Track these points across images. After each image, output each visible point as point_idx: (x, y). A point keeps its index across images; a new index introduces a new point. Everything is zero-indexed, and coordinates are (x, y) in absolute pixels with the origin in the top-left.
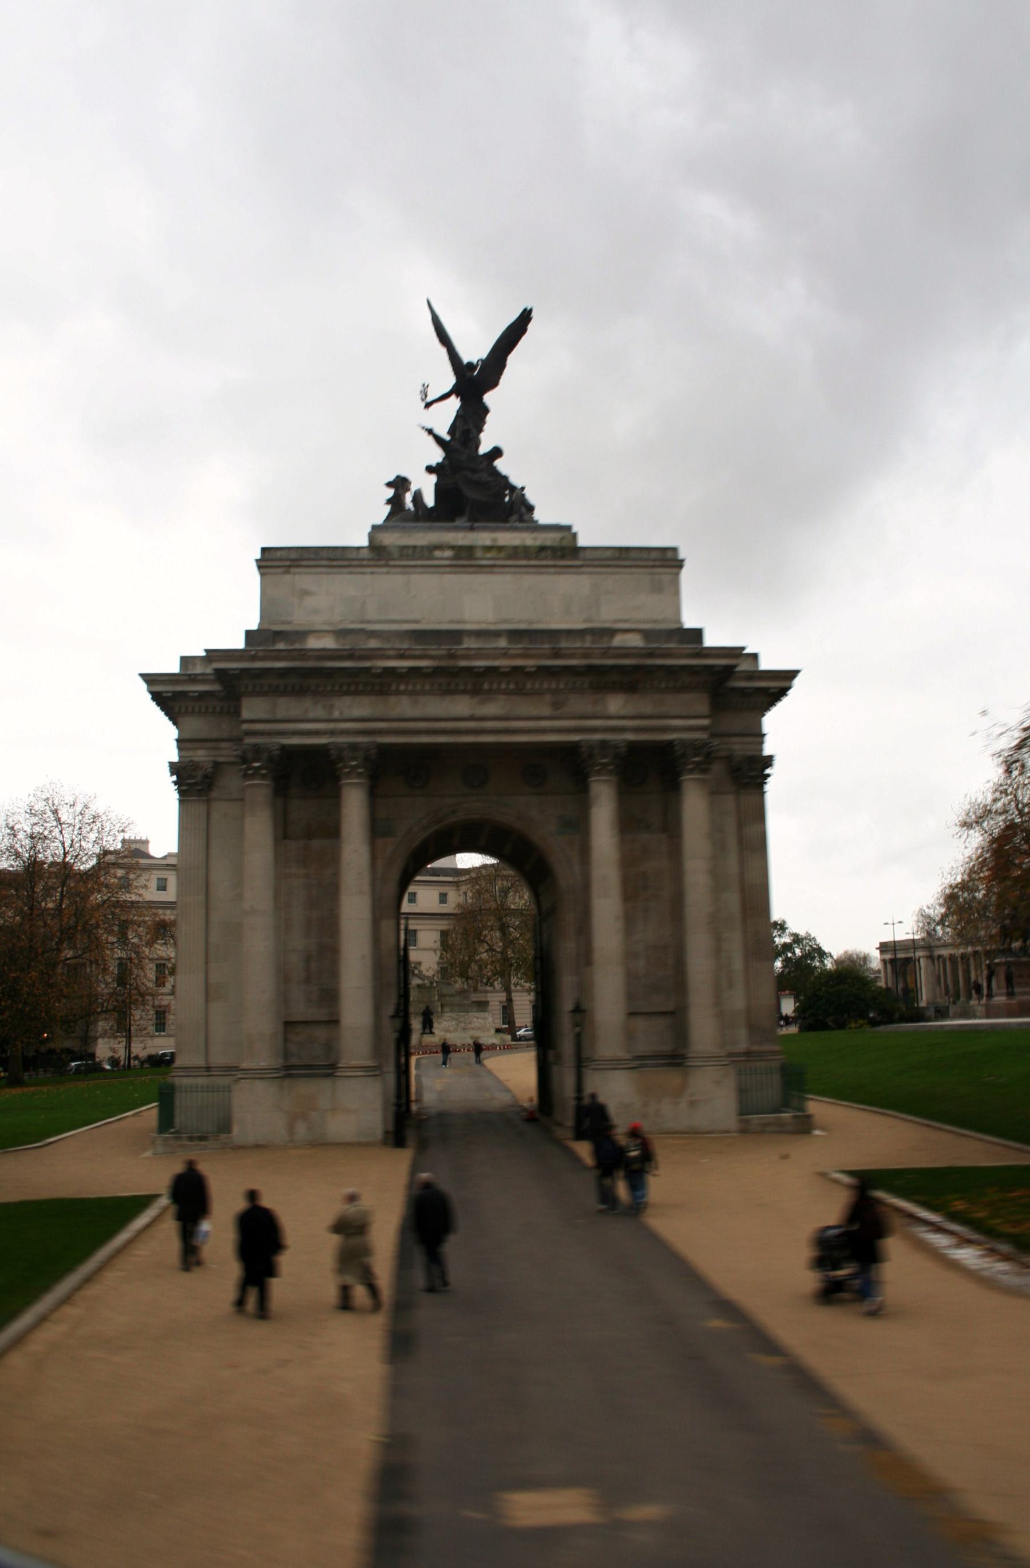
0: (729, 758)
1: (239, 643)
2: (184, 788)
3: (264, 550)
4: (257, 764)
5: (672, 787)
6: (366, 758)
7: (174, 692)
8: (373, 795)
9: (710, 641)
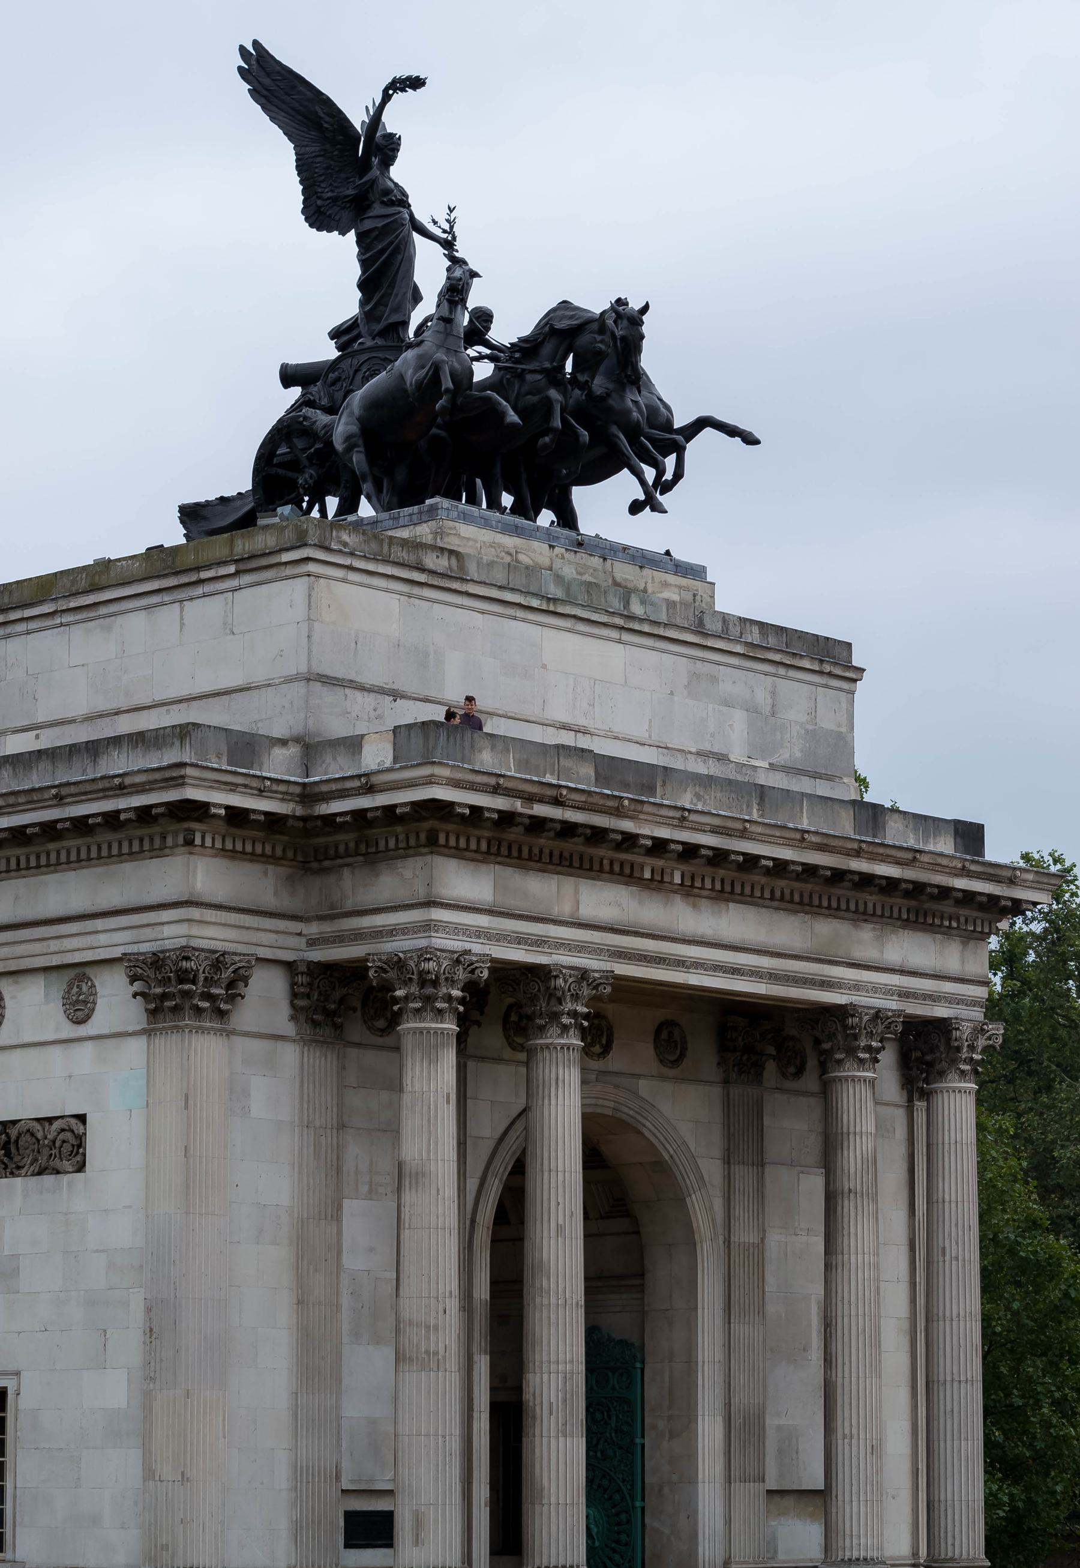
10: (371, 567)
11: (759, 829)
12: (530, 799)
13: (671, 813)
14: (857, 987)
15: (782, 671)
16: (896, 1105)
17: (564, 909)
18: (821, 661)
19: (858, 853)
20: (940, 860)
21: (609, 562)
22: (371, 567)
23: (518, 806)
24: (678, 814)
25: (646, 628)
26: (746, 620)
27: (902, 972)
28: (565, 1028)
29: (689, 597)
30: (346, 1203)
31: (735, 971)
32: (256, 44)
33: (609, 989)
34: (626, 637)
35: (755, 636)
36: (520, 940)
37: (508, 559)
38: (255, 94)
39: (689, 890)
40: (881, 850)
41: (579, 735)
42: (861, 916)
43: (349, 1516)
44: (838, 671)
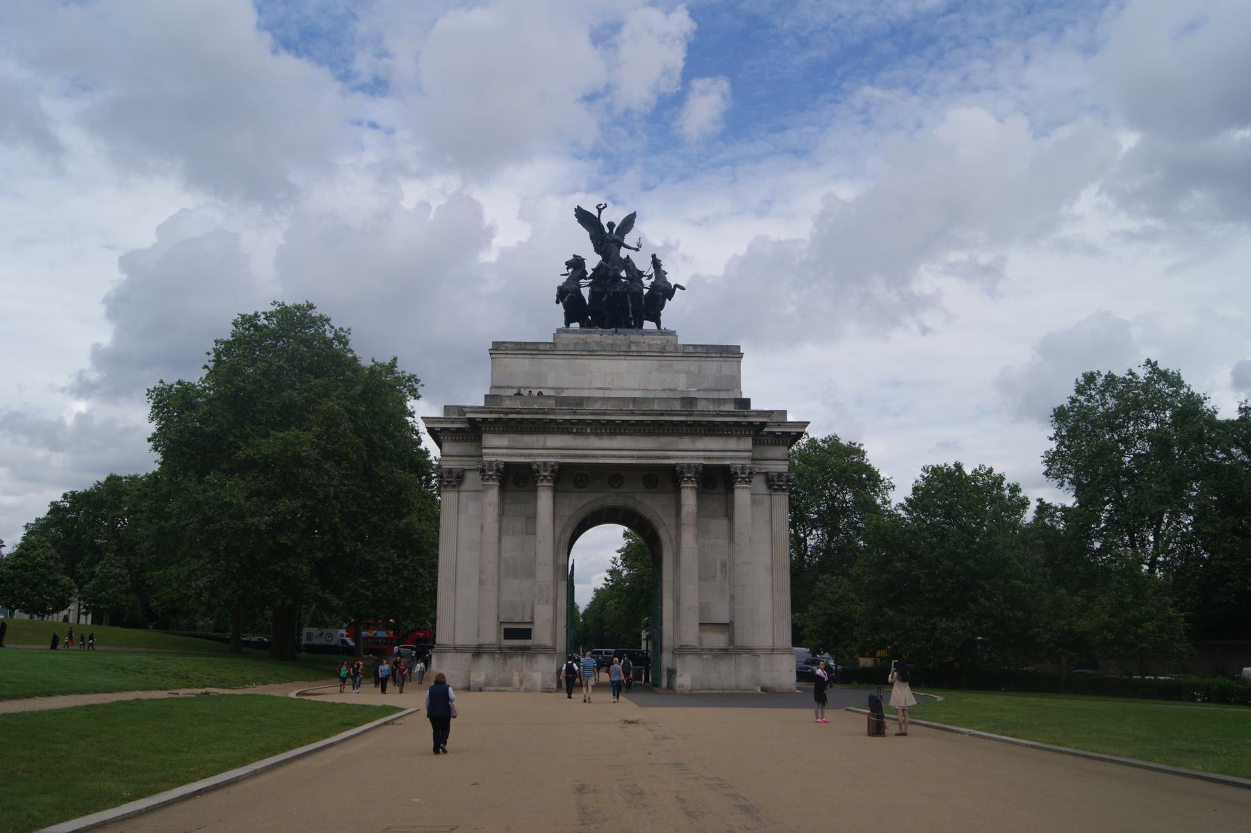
0: (767, 474)
1: (482, 404)
2: (445, 484)
3: (494, 343)
4: (490, 473)
5: (730, 490)
6: (553, 471)
7: (441, 428)
8: (555, 490)
9: (753, 407)
10: (515, 352)
11: (611, 412)
12: (507, 413)
13: (568, 411)
14: (683, 457)
15: (703, 359)
16: (764, 494)
17: (541, 445)
18: (721, 353)
19: (662, 415)
20: (703, 413)
21: (627, 336)
22: (515, 352)
23: (502, 416)
24: (571, 411)
25: (635, 354)
26: (686, 345)
27: (704, 451)
28: (542, 480)
29: (666, 341)
30: (503, 538)
31: (620, 457)
32: (578, 206)
33: (557, 467)
34: (627, 358)
35: (691, 350)
36: (521, 455)
37: (582, 342)
38: (579, 221)
39: (597, 434)
40: (672, 412)
41: (606, 391)
42: (681, 434)
43: (505, 629)
44: (731, 356)
